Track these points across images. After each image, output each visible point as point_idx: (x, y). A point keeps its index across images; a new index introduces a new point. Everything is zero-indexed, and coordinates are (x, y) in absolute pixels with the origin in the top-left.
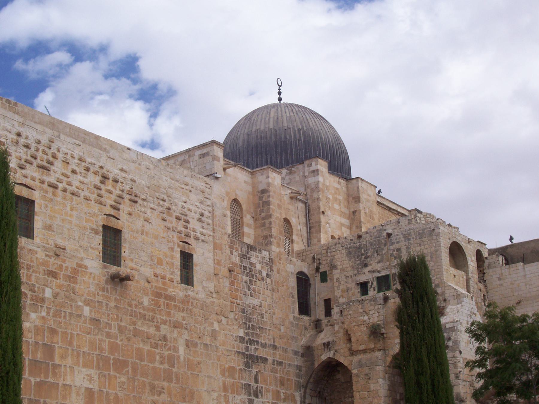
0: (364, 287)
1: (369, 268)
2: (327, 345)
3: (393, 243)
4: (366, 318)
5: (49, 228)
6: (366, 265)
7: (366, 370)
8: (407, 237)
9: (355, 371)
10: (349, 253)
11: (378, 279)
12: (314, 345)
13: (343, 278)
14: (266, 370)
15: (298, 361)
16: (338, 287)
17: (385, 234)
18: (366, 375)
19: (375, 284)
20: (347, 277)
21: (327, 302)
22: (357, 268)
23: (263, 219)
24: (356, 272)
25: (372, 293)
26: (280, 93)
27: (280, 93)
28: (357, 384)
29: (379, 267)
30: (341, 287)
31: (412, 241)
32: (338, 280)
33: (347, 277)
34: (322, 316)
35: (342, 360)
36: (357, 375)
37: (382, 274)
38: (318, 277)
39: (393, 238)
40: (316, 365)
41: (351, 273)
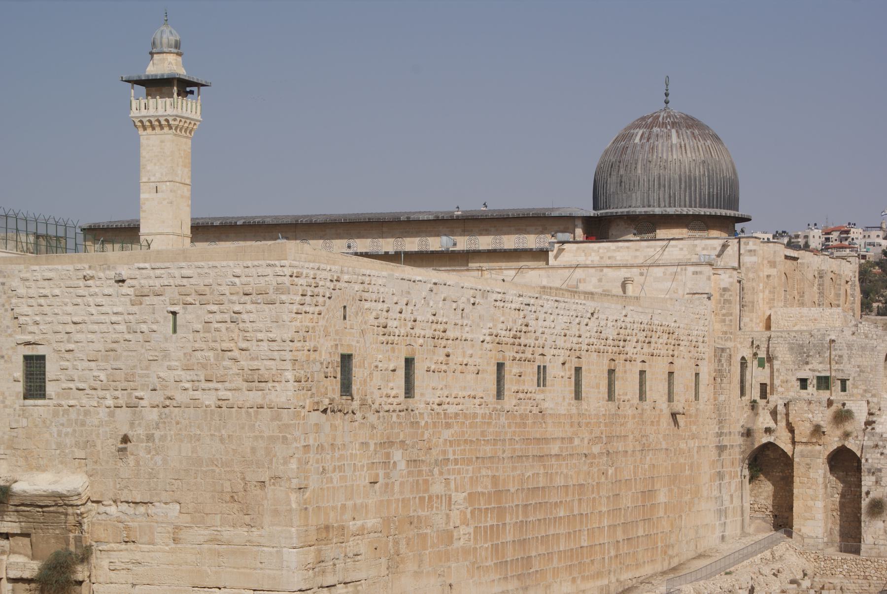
0: (804, 383)
1: (810, 366)
2: (768, 430)
3: (835, 350)
4: (810, 416)
5: (651, 390)
6: (807, 363)
7: (808, 460)
8: (850, 347)
9: (796, 460)
10: (791, 349)
11: (819, 378)
12: (755, 428)
13: (783, 370)
14: (725, 455)
15: (739, 440)
16: (778, 377)
17: (828, 339)
18: (807, 464)
19: (815, 381)
20: (787, 370)
21: (763, 386)
22: (798, 364)
23: (724, 315)
24: (796, 367)
25: (811, 389)
26: (667, 95)
27: (667, 95)
28: (798, 471)
29: (820, 367)
30: (781, 377)
31: (854, 352)
32: (778, 370)
33: (787, 370)
34: (758, 399)
35: (782, 446)
36: (799, 463)
37: (823, 374)
38: (756, 362)
39: (837, 345)
40: (756, 446)
41: (792, 367)
